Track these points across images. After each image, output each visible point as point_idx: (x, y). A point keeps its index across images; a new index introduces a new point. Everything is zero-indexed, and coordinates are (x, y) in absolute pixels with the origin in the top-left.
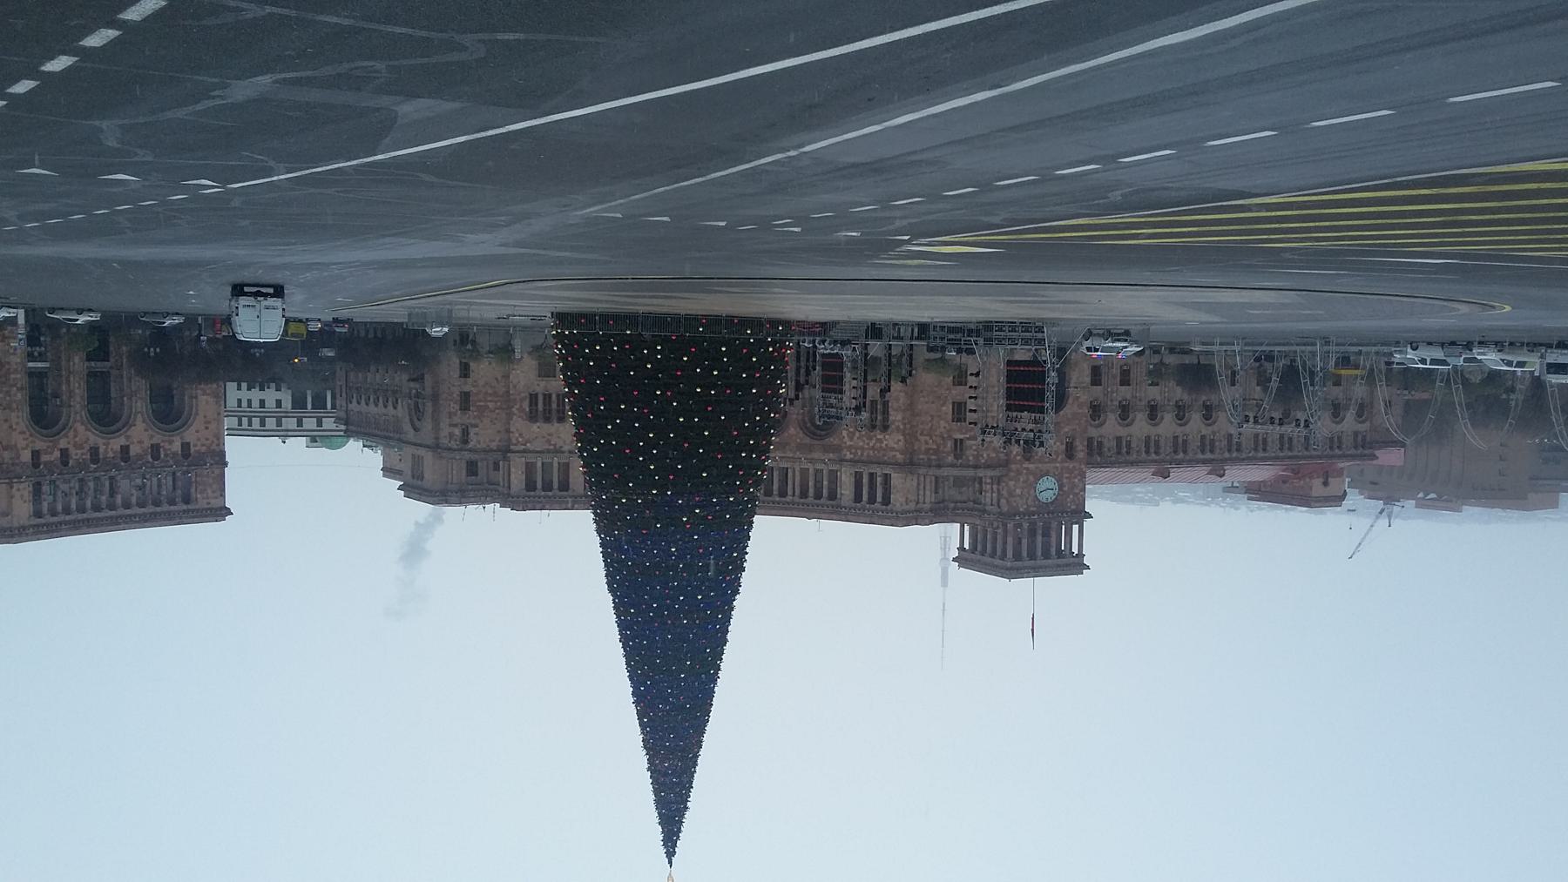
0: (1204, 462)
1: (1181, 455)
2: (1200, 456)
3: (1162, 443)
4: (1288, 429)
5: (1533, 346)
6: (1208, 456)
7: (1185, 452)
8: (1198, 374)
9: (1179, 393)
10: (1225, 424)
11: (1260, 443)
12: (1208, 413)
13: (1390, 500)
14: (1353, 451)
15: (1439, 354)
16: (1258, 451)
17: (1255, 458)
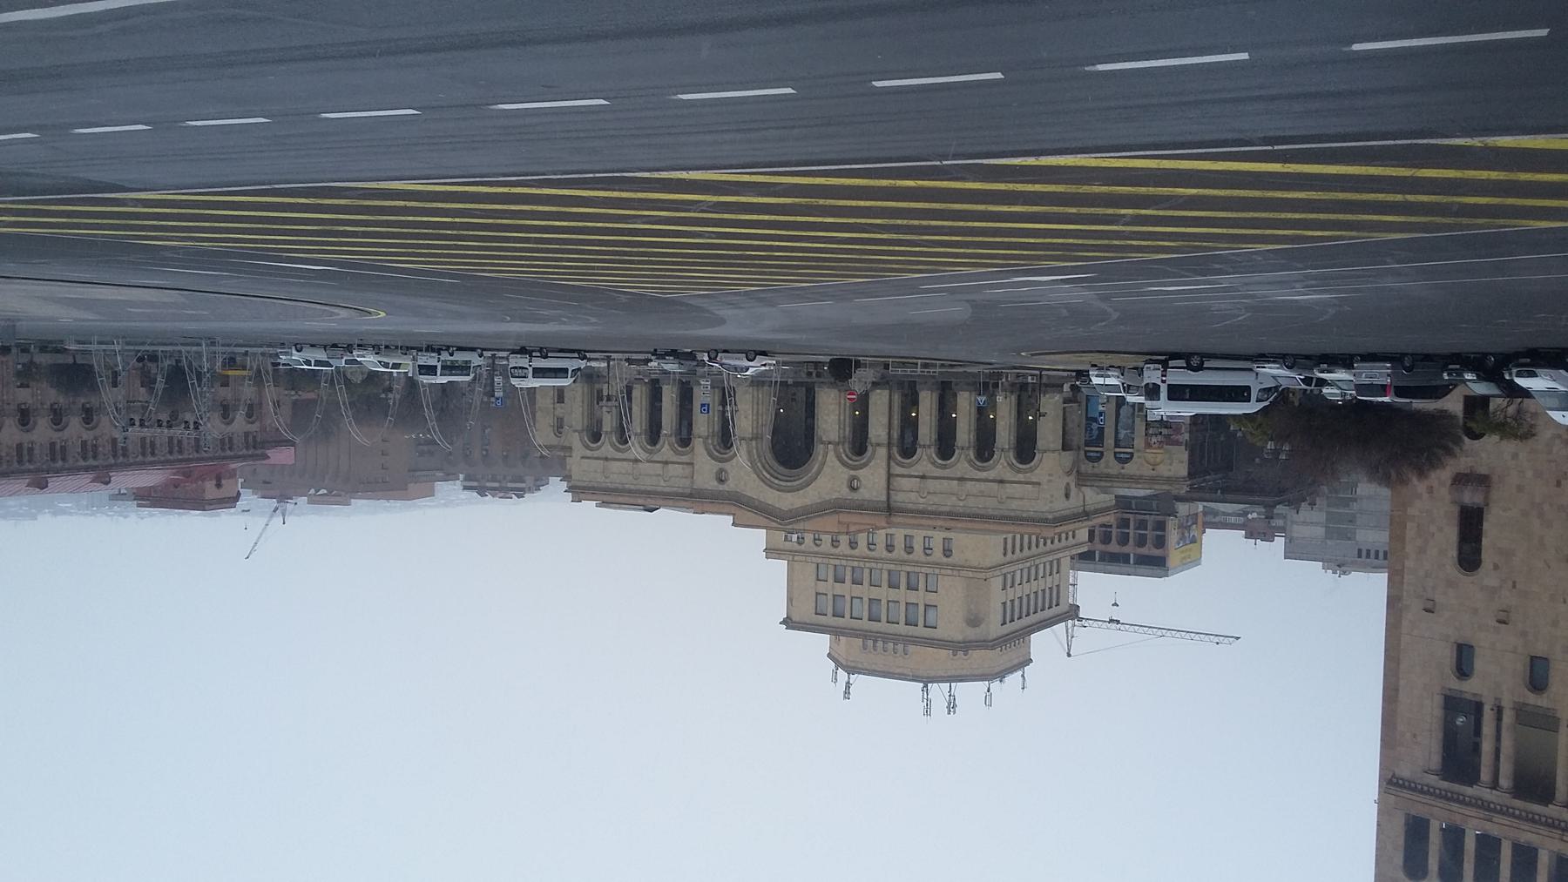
0: (87, 469)
1: (60, 464)
2: (82, 463)
3: (36, 452)
4: (177, 432)
5: (406, 350)
6: (91, 462)
7: (64, 459)
8: (75, 375)
9: (52, 395)
10: (109, 428)
11: (147, 448)
12: (88, 415)
13: (283, 498)
14: (244, 452)
15: (321, 355)
16: (146, 455)
17: (143, 464)
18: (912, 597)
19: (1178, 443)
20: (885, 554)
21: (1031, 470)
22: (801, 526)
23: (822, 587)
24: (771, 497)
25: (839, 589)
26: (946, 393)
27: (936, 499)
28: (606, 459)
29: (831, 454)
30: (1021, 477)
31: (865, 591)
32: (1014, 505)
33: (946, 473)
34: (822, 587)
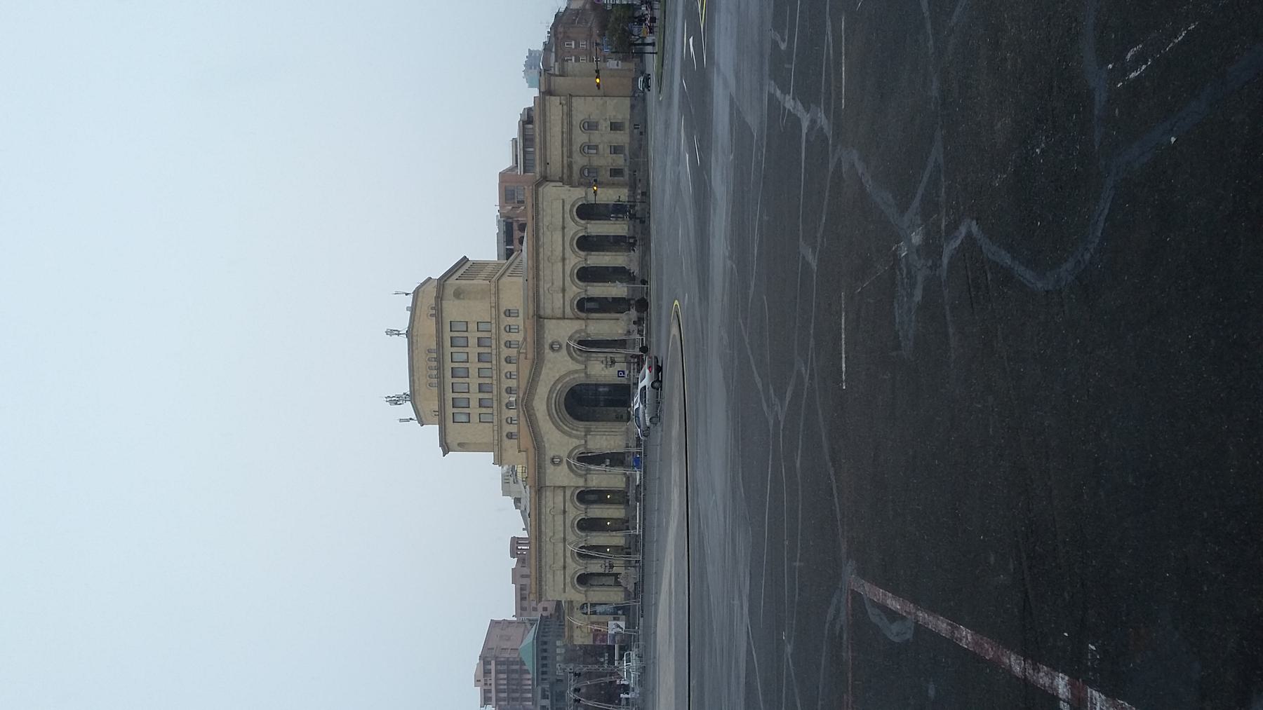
18: (474, 403)
19: (595, 640)
20: (504, 386)
21: (573, 586)
22: (522, 419)
23: (473, 327)
24: (542, 390)
25: (473, 342)
26: (622, 525)
27: (550, 518)
28: (564, 228)
29: (575, 442)
30: (568, 580)
31: (474, 367)
32: (549, 576)
33: (569, 530)
34: (473, 327)
